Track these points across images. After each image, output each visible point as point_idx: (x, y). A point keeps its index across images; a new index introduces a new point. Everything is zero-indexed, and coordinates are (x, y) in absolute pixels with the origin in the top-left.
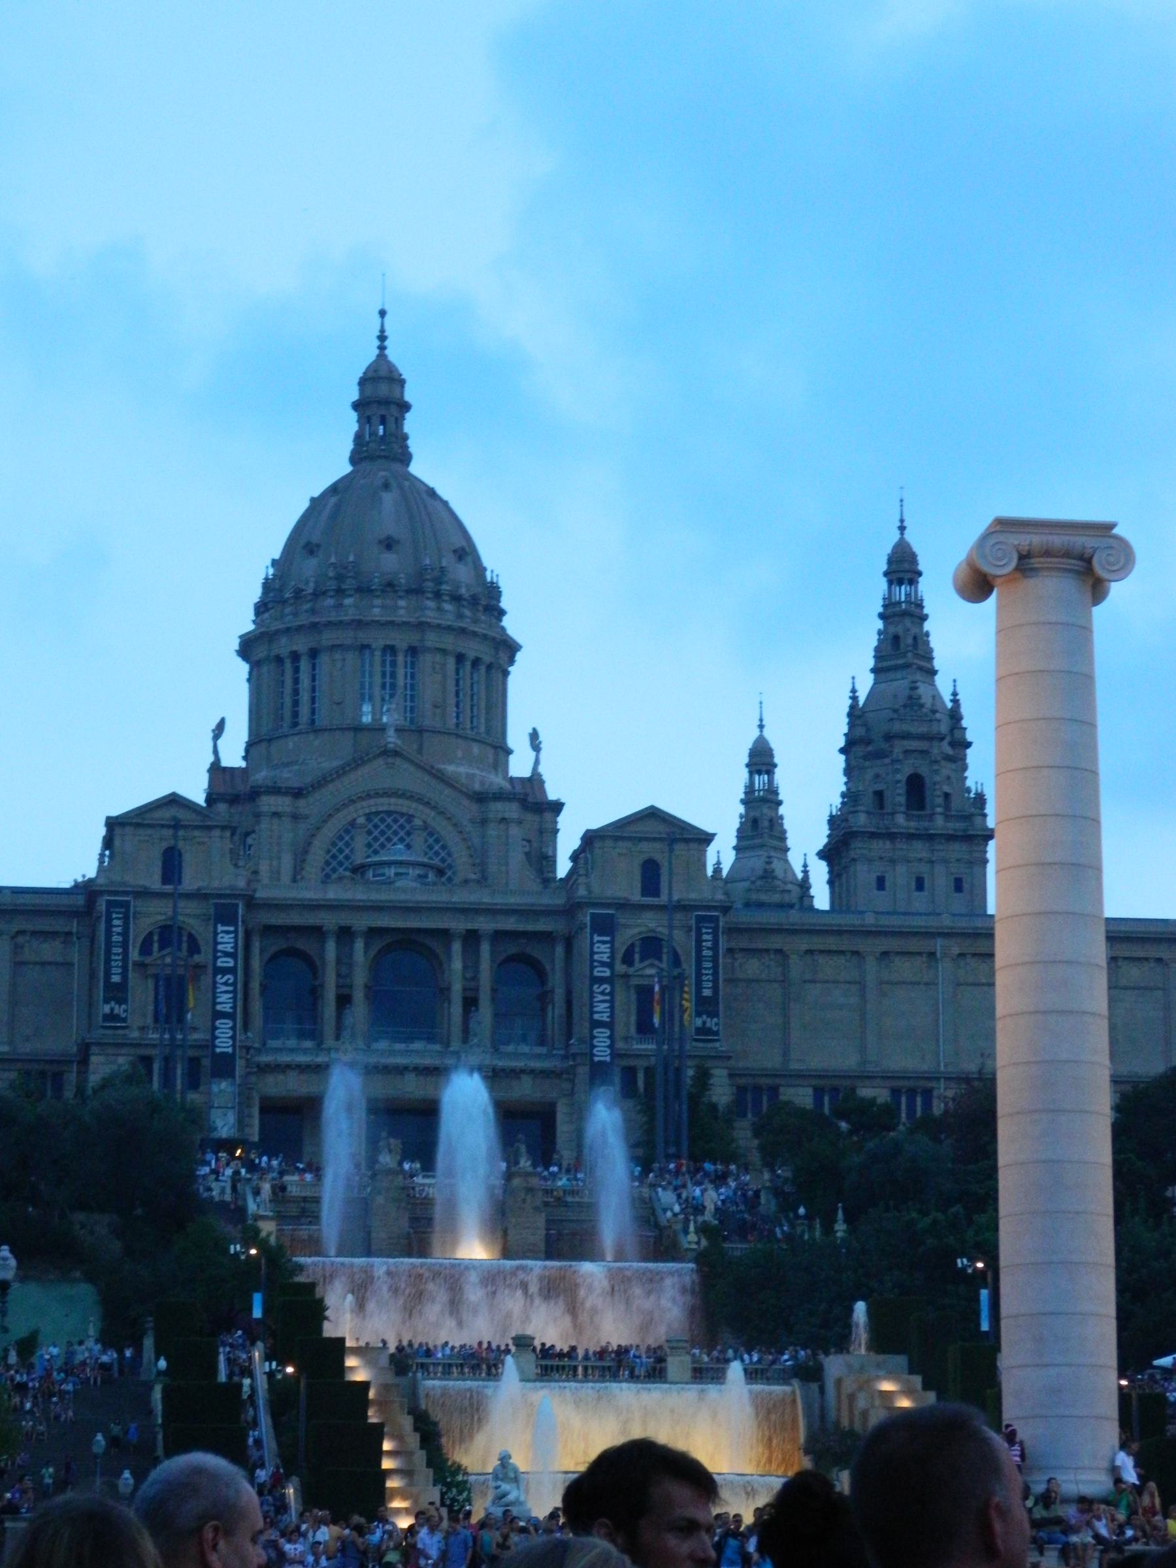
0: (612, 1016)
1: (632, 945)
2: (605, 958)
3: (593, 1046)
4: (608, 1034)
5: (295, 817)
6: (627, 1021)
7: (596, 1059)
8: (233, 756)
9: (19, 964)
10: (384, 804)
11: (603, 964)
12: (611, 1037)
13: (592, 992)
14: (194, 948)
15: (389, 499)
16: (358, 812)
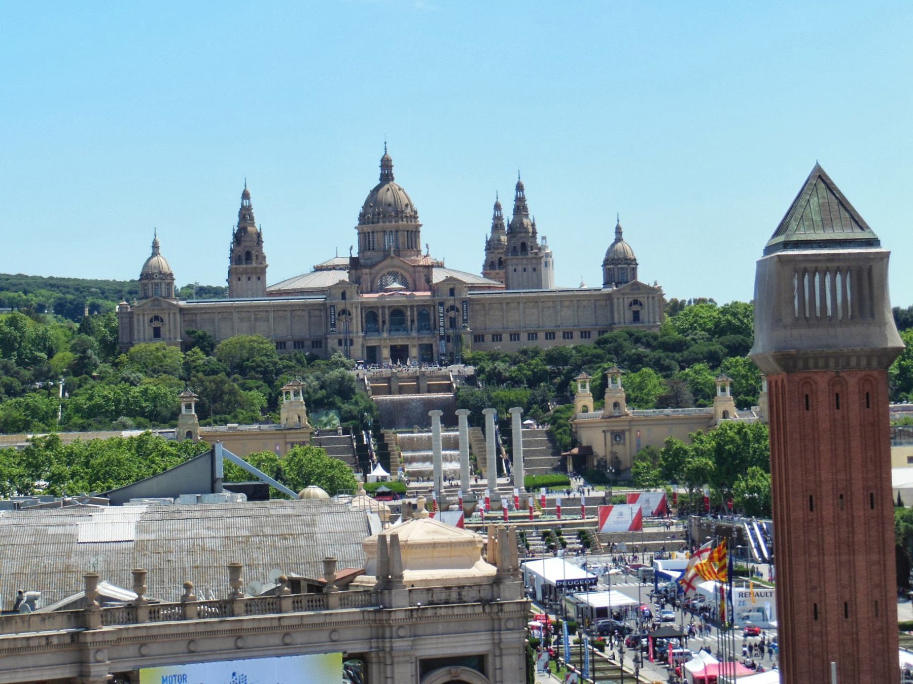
5: (371, 274)
6: (448, 324)
8: (355, 255)
9: (310, 317)
10: (391, 270)
14: (350, 314)
15: (389, 193)
16: (385, 272)
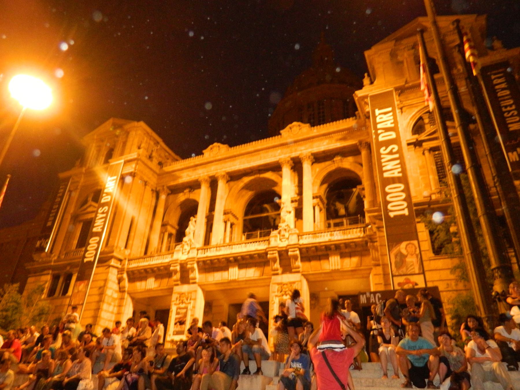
0: (404, 171)
1: (421, 118)
2: (389, 125)
3: (387, 203)
4: (402, 186)
7: (392, 215)
11: (387, 130)
12: (407, 190)
13: (379, 154)
